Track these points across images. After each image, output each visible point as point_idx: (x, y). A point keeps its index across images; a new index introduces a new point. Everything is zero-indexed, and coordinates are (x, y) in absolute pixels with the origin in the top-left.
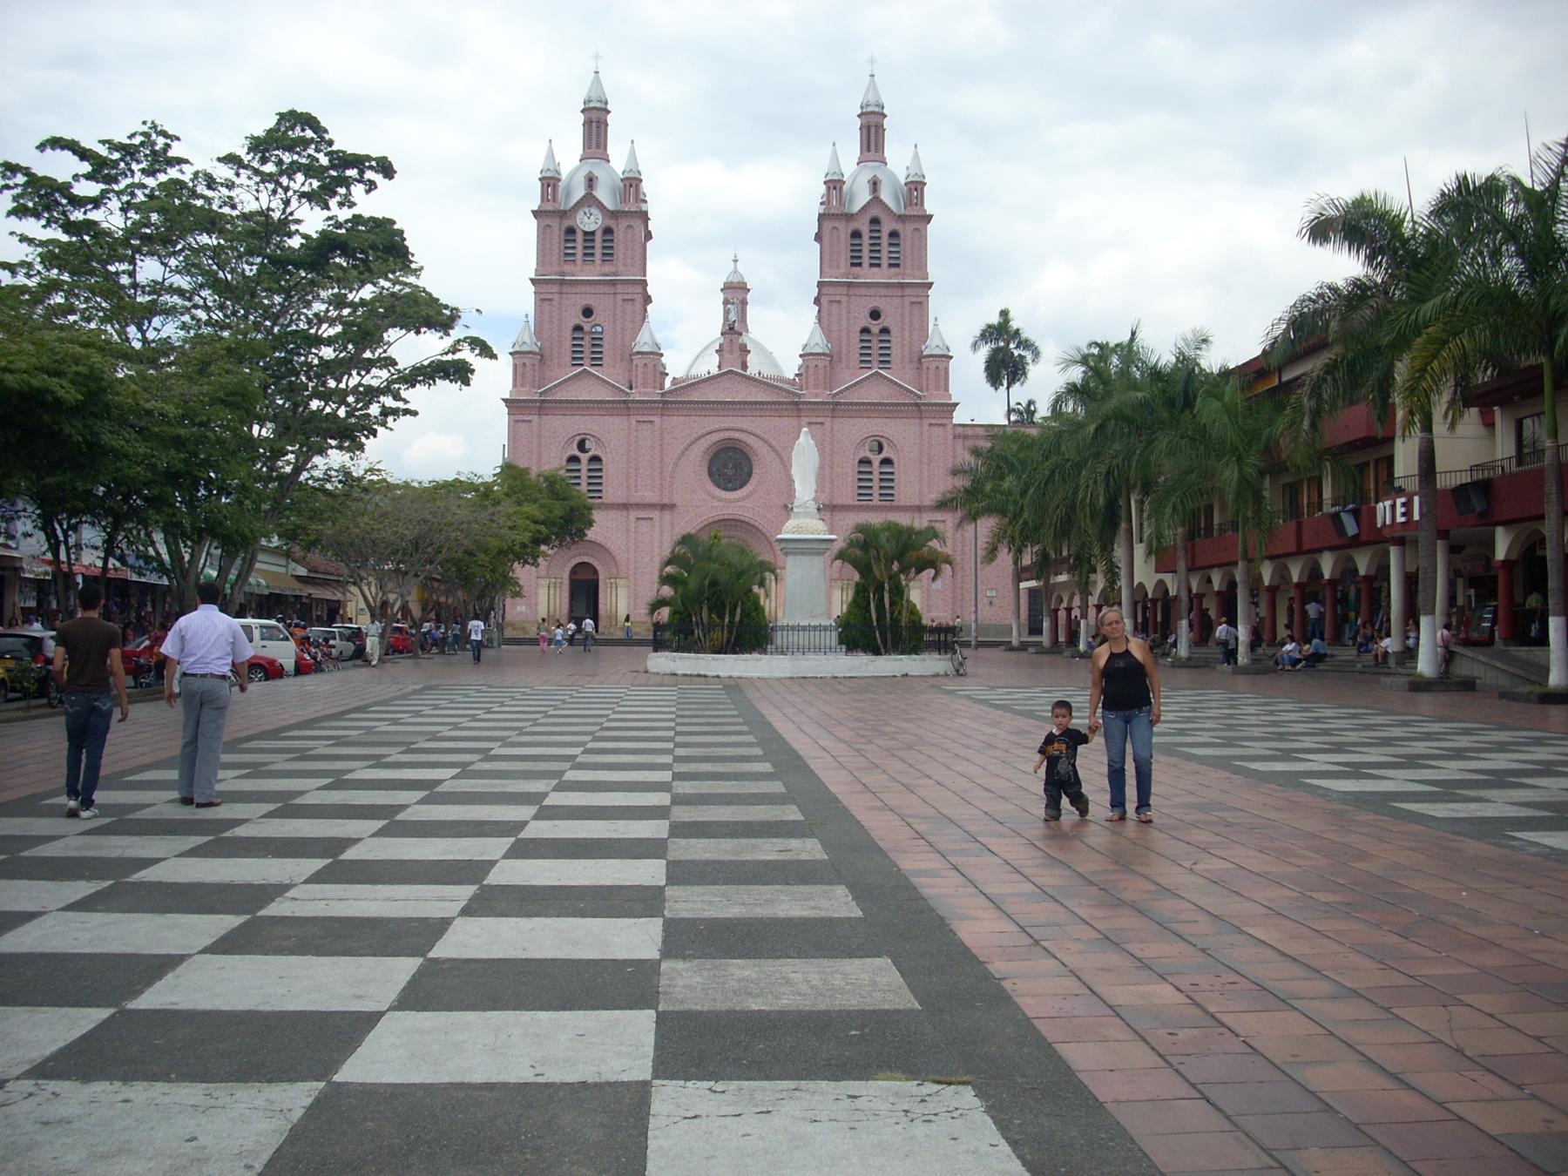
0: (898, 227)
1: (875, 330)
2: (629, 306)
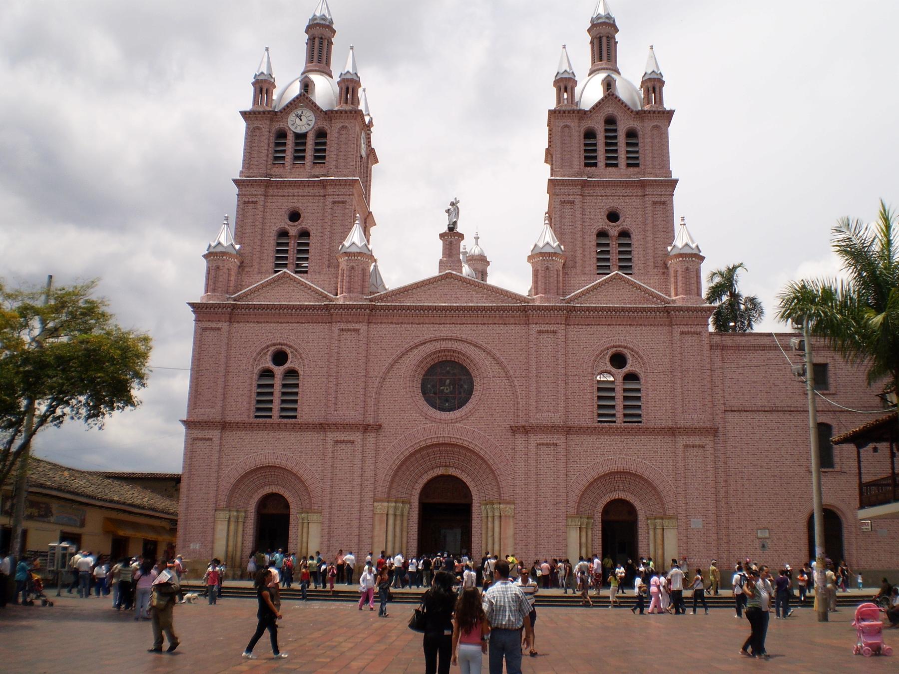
0: (636, 125)
1: (614, 230)
2: (339, 209)
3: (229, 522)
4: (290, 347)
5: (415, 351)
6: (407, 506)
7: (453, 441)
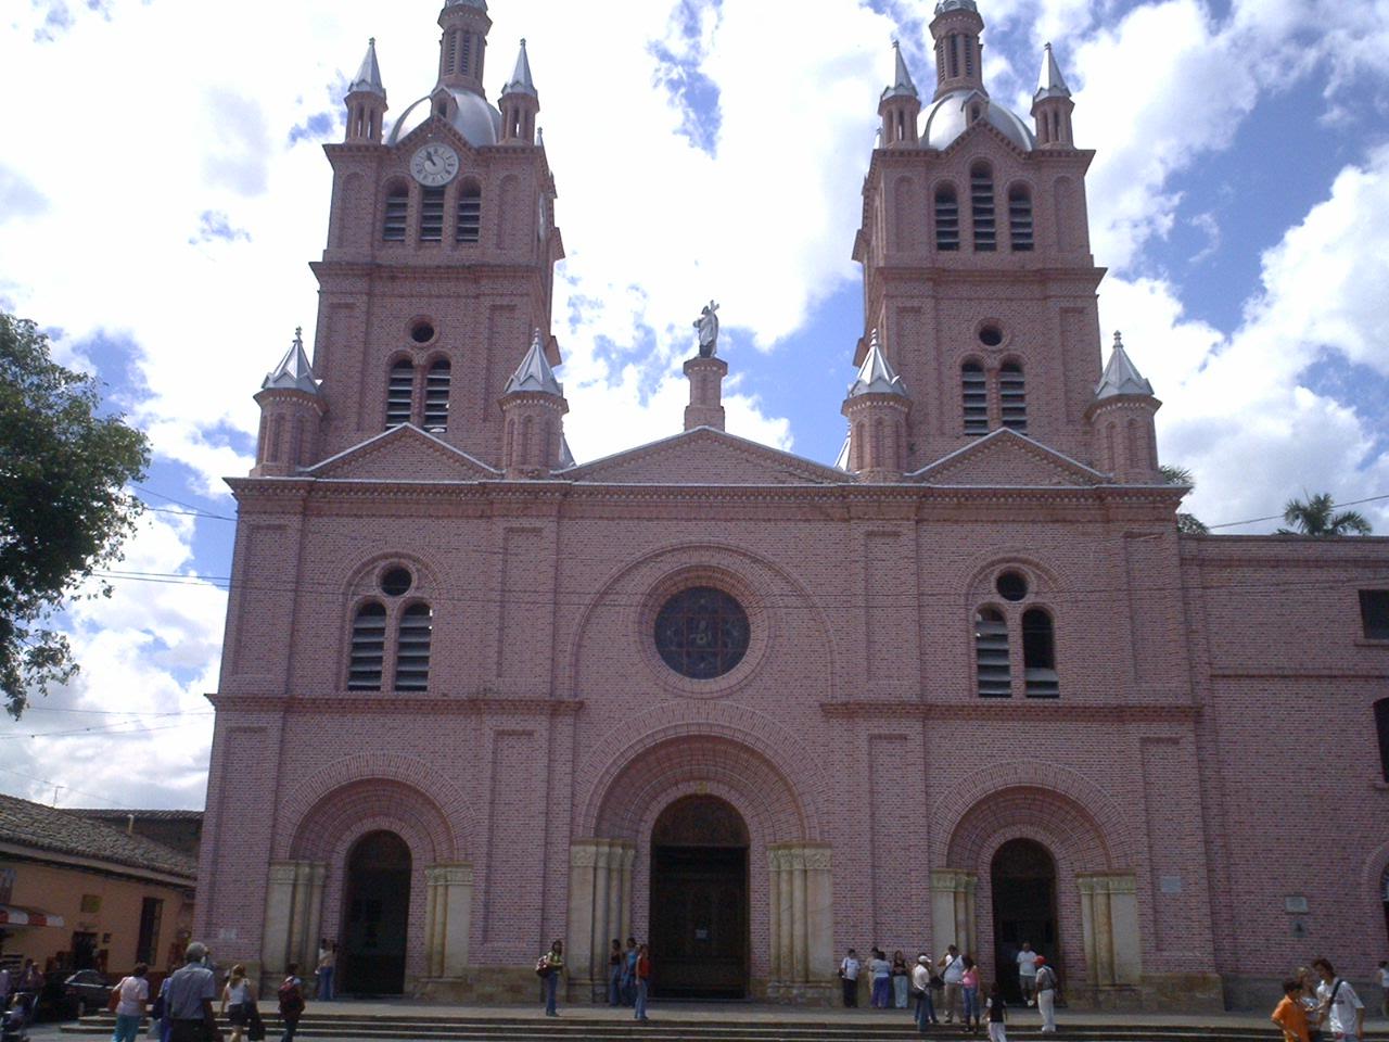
1: (992, 358)
3: (295, 886)
4: (416, 560)
5: (644, 570)
6: (631, 852)
7: (716, 732)
